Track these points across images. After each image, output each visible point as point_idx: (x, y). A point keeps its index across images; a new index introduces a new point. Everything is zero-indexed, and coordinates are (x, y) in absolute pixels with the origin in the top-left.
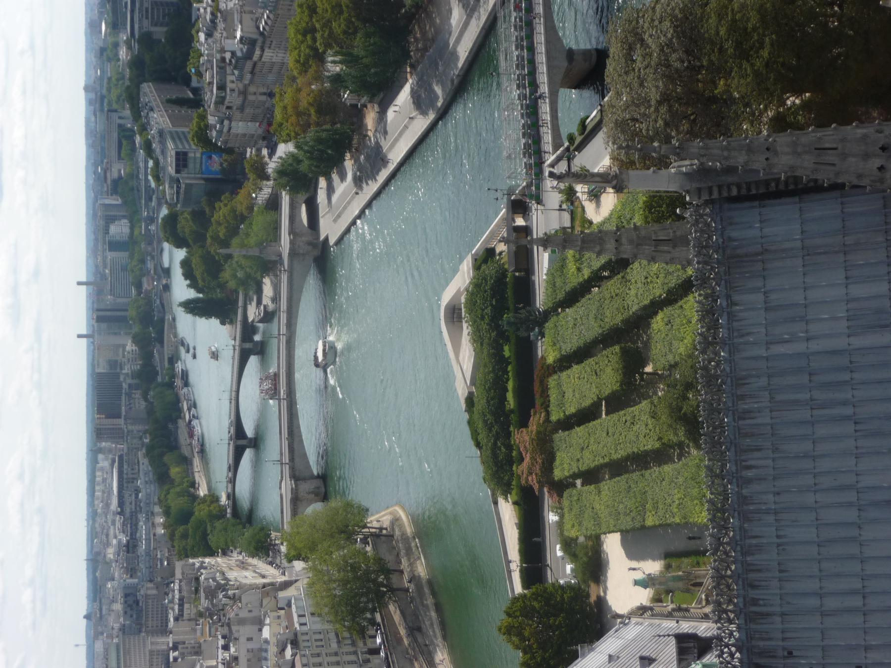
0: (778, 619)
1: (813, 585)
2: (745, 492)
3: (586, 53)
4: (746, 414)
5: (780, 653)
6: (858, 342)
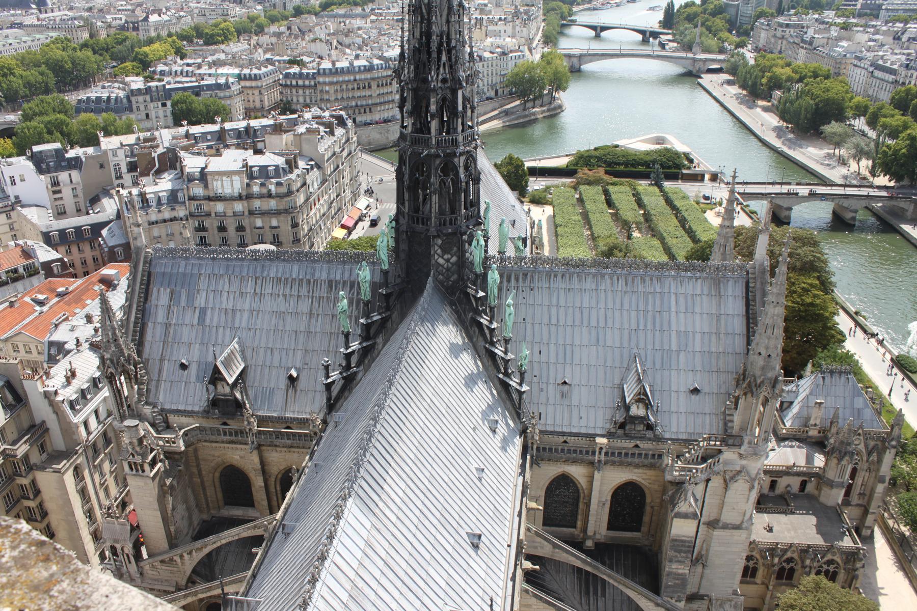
0: (547, 285)
1: (562, 303)
2: (607, 277)
3: (789, 217)
4: (643, 280)
5: (532, 285)
6: (674, 335)
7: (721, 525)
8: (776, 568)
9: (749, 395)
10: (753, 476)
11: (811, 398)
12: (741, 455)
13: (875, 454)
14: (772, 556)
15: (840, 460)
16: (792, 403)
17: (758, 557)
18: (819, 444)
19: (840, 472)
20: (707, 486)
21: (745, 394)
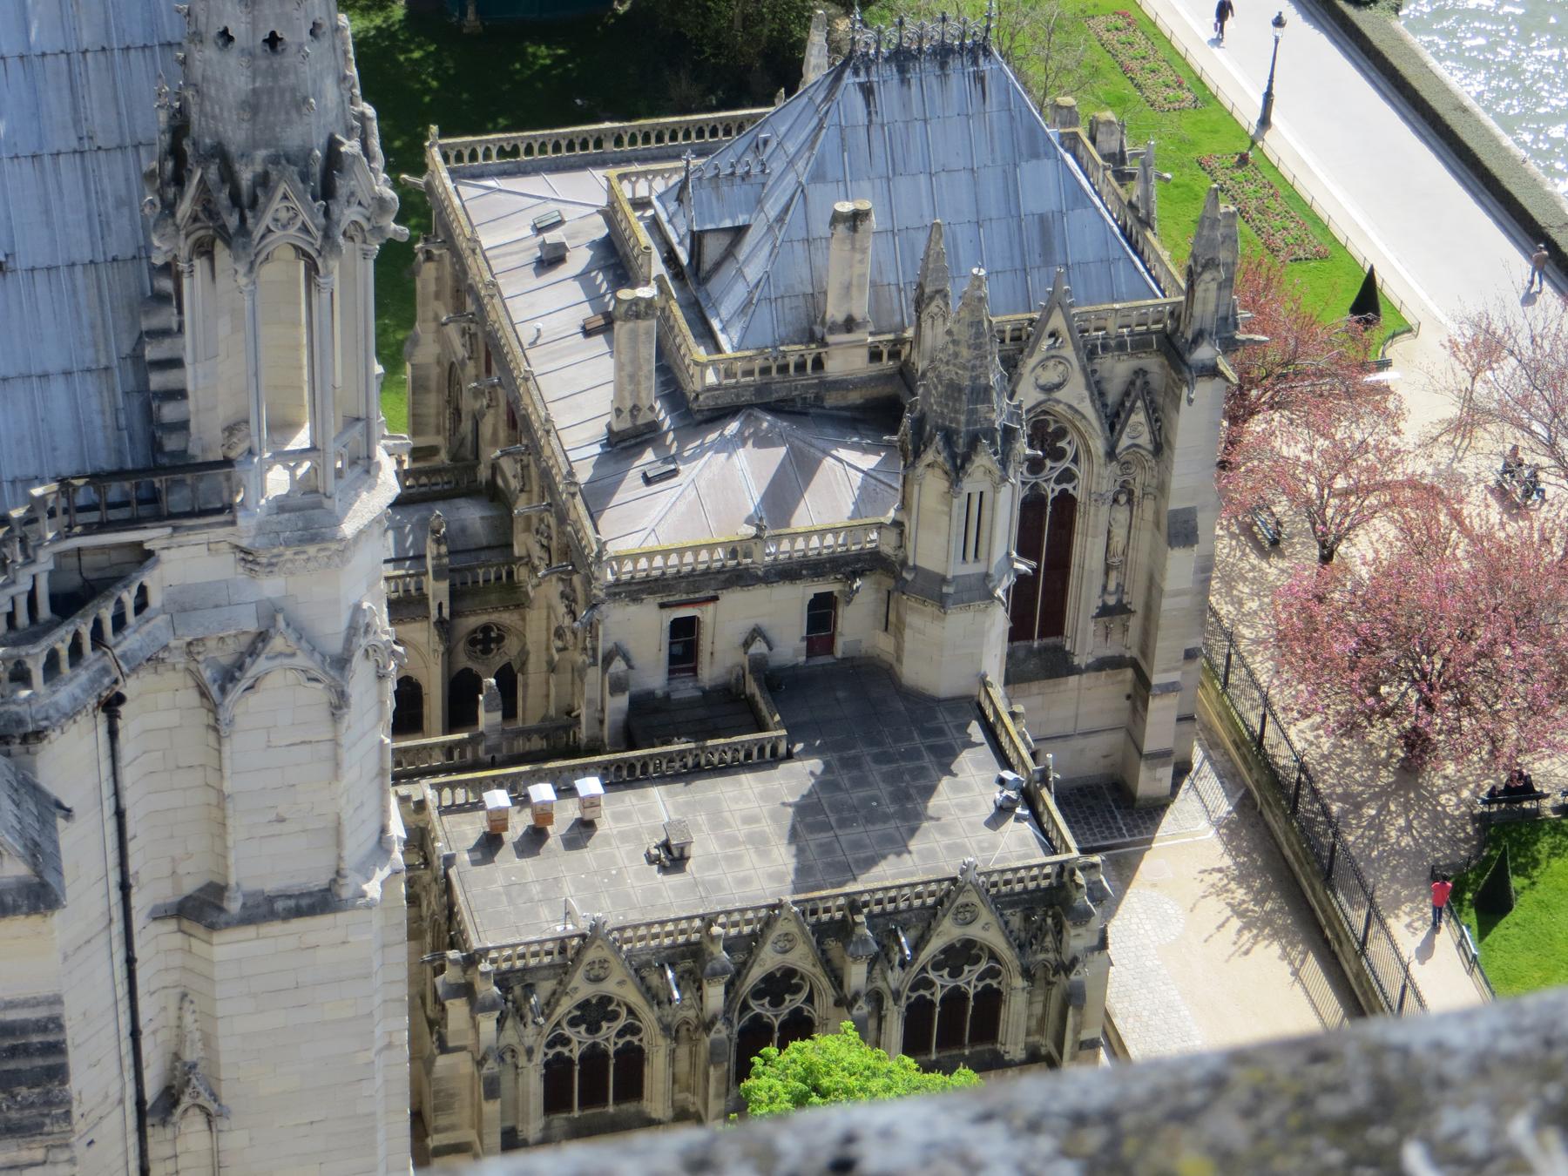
7: (234, 906)
8: (721, 1032)
9: (222, 253)
10: (336, 646)
11: (816, 192)
12: (246, 556)
13: (1139, 417)
14: (693, 980)
15: (957, 468)
16: (739, 232)
17: (632, 996)
18: (880, 413)
19: (970, 525)
20: (113, 733)
21: (204, 249)
